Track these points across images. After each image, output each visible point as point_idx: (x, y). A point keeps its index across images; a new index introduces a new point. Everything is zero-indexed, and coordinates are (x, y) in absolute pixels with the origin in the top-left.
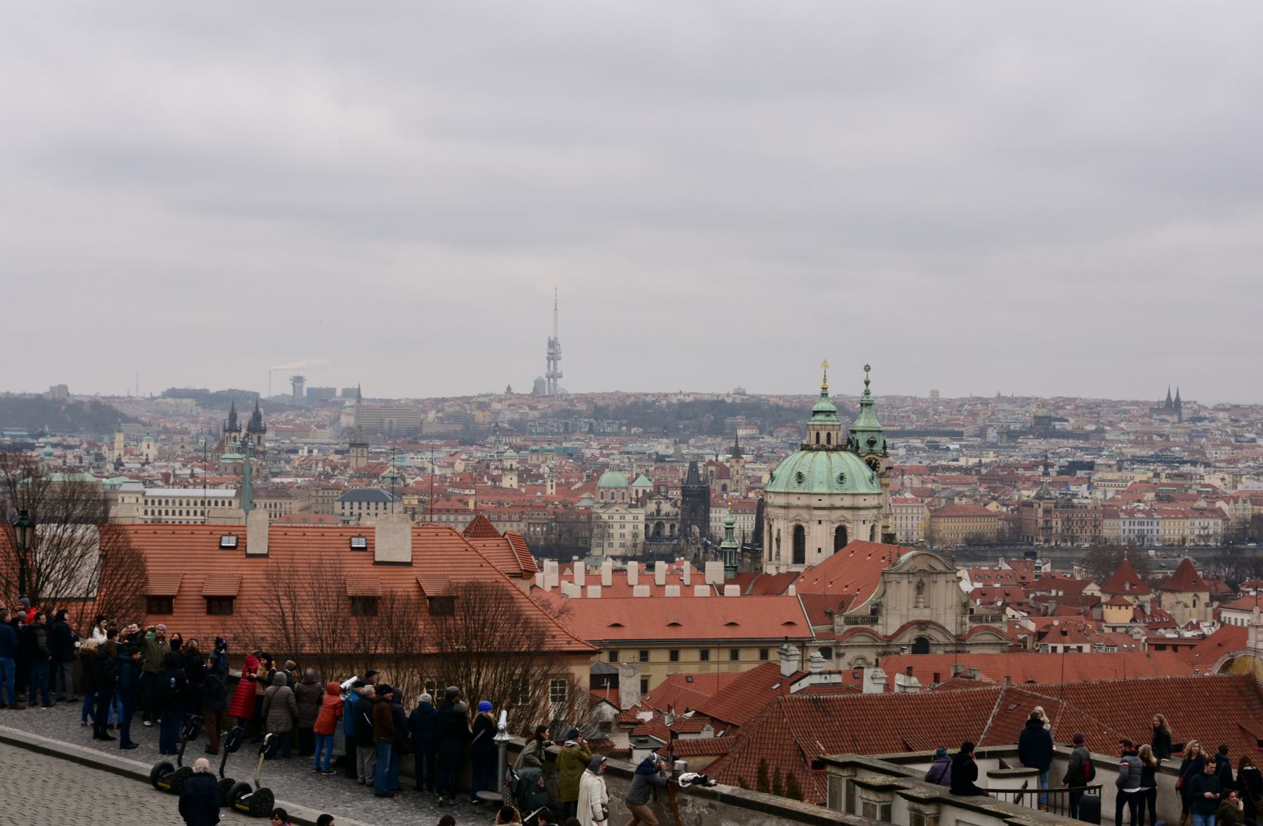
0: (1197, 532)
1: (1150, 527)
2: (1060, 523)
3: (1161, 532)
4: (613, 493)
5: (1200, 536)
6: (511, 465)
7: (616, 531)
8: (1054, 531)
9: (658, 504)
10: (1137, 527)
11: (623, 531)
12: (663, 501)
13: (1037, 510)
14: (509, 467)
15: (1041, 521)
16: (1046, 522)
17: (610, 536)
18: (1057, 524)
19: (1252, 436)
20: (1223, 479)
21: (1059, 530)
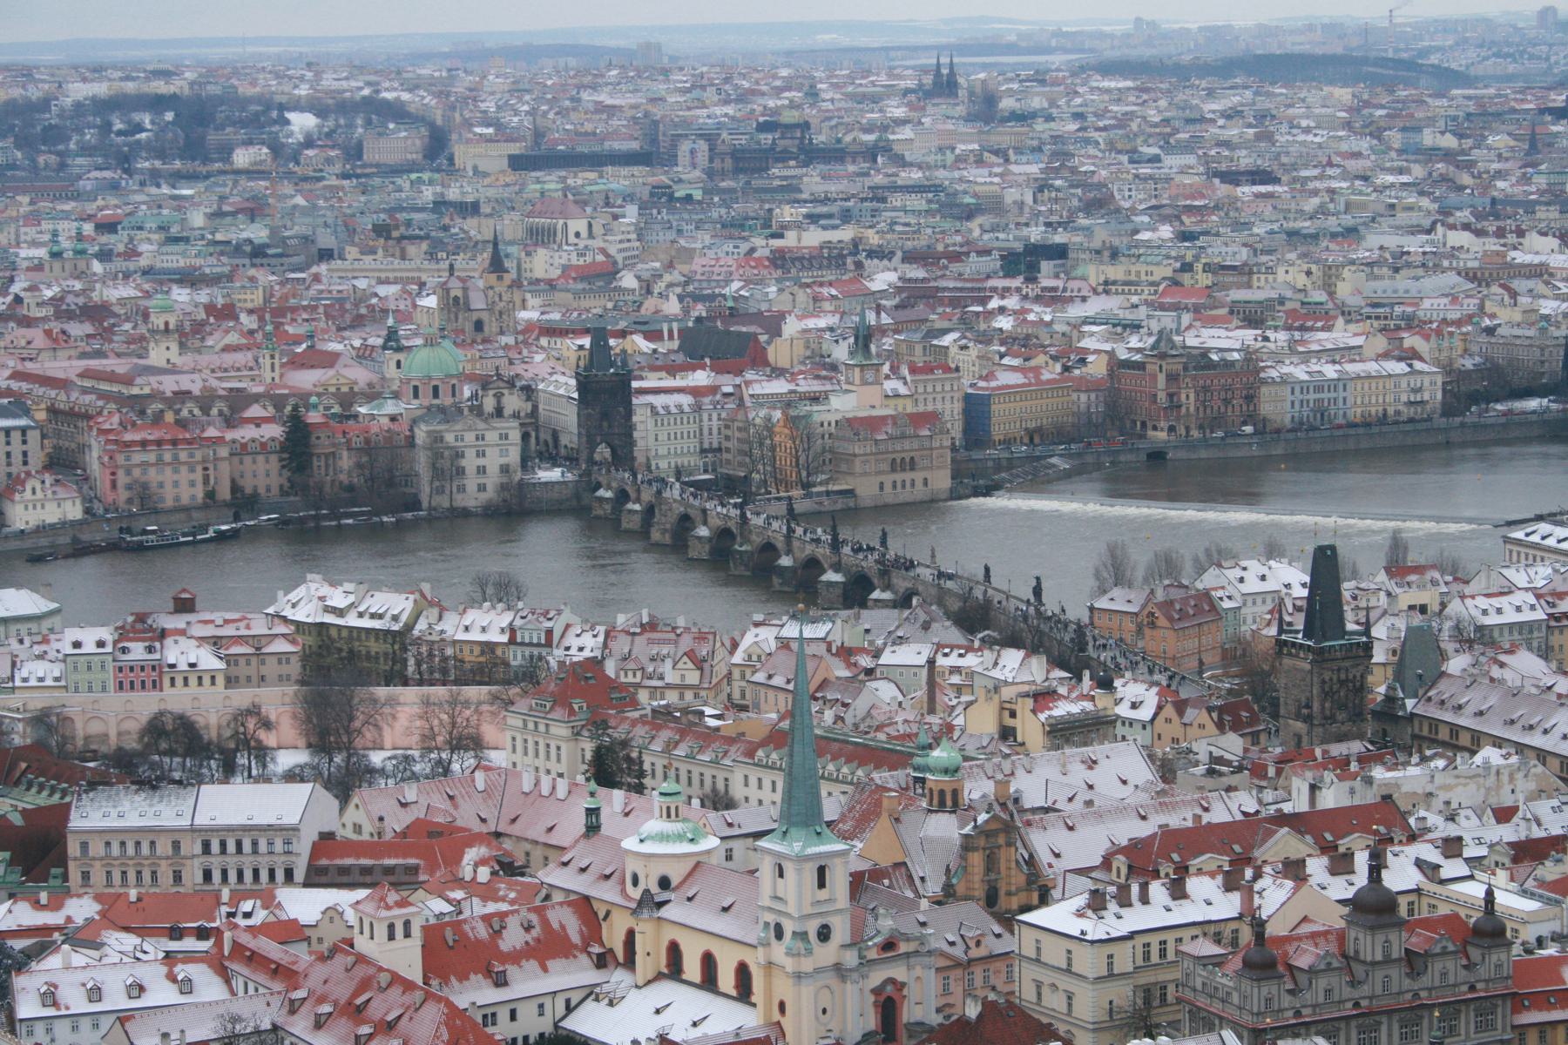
0: (1404, 398)
1: (1333, 395)
2: (1192, 396)
3: (1350, 401)
4: (436, 389)
5: (1410, 403)
6: (167, 324)
7: (470, 462)
8: (1183, 410)
9: (498, 397)
10: (1312, 396)
11: (481, 462)
12: (506, 392)
13: (1154, 377)
14: (162, 327)
15: (1162, 396)
16: (1171, 396)
17: (461, 472)
18: (1188, 398)
19: (1154, 150)
20: (1309, 273)
21: (1192, 409)
